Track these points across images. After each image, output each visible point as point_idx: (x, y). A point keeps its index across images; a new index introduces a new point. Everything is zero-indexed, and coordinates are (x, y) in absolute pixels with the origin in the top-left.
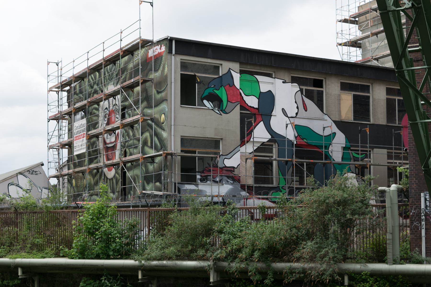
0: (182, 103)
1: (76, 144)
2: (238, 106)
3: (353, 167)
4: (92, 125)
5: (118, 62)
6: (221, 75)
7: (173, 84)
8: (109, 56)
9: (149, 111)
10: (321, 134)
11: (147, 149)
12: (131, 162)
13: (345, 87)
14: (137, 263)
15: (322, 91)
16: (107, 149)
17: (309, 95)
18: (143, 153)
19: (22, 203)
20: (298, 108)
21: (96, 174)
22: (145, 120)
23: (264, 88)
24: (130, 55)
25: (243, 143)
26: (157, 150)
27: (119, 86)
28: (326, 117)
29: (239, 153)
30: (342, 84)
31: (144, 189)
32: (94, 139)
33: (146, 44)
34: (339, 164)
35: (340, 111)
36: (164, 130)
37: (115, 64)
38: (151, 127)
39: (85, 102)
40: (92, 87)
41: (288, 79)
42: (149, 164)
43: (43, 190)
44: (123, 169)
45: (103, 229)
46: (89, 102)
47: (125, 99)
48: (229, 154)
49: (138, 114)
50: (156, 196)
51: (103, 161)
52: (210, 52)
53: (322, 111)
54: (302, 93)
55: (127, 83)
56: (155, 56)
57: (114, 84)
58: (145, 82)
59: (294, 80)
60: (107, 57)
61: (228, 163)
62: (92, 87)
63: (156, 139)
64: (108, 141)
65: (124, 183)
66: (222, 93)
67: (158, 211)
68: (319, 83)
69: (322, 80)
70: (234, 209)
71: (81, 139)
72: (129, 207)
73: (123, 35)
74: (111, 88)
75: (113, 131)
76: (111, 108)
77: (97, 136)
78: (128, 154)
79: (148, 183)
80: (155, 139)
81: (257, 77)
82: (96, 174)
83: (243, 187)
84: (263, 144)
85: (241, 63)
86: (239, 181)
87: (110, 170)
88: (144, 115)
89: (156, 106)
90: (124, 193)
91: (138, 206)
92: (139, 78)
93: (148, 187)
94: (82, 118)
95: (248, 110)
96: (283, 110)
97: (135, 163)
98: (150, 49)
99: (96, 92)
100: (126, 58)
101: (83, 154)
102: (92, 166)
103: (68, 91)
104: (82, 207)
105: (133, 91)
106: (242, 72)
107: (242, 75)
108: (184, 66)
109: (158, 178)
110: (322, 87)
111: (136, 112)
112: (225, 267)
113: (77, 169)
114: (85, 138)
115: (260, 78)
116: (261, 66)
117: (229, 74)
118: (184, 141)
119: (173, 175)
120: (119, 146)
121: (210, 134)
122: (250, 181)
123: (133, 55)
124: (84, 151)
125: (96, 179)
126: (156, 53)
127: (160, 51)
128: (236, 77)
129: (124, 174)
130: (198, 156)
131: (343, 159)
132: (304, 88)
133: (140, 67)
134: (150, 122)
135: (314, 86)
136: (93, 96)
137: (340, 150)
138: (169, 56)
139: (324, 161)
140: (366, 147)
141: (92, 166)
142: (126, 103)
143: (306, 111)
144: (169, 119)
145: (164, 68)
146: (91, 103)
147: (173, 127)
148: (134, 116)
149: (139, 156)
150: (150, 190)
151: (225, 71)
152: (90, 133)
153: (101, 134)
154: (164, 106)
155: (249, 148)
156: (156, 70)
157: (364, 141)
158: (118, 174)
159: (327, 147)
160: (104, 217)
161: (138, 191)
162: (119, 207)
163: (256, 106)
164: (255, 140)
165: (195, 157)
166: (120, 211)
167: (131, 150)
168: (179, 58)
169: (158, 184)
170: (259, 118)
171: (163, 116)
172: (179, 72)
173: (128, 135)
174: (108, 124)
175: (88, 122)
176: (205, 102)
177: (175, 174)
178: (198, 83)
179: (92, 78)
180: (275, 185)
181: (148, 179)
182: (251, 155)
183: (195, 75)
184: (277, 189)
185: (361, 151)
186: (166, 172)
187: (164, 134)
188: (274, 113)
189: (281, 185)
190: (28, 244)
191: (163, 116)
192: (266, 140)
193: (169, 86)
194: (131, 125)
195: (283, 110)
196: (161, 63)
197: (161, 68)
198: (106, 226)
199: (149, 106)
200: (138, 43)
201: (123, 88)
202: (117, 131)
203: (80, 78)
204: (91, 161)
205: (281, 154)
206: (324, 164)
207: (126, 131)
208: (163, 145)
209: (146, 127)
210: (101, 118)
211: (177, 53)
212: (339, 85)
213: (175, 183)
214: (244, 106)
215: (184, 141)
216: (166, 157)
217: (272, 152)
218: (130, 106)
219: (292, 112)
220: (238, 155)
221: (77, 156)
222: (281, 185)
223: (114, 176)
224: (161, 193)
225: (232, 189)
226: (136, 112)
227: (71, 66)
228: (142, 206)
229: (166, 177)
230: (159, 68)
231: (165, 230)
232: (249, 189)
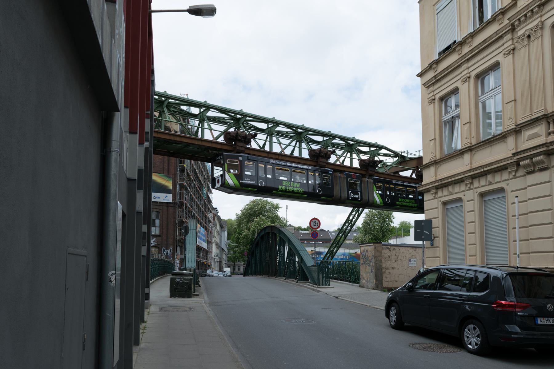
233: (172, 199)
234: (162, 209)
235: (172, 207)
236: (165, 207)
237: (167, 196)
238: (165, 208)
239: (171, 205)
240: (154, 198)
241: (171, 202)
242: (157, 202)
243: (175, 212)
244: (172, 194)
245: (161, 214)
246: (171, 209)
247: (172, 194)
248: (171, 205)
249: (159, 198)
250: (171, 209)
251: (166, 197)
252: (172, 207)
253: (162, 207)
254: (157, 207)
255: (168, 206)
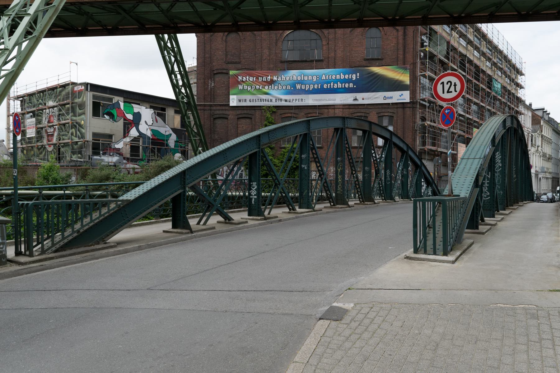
0: (93, 116)
1: (28, 131)
2: (123, 119)
3: (180, 151)
4: (39, 122)
5: (56, 90)
6: (113, 103)
7: (88, 106)
8: (51, 86)
9: (74, 118)
10: (164, 134)
11: (73, 137)
12: (64, 143)
13: (176, 112)
14: (71, 192)
15: (165, 114)
16: (48, 136)
17: (159, 115)
18: (72, 140)
19: (3, 163)
20: (153, 121)
21: (41, 148)
22: (72, 123)
23: (136, 111)
24: (63, 88)
25: (124, 137)
26: (79, 138)
27: (57, 104)
28: (167, 126)
29: (122, 142)
30: (175, 110)
31: (71, 157)
32: (39, 129)
33: (73, 84)
34: (173, 149)
35: (174, 124)
36: (83, 128)
37: (53, 91)
38: (76, 127)
39: (34, 109)
40: (38, 101)
41: (148, 106)
42: (74, 145)
43: (4, 155)
44: (59, 146)
45: (52, 176)
46: (37, 109)
47: (60, 110)
48: (118, 142)
49: (68, 119)
50: (81, 161)
51: (45, 142)
52: (108, 91)
53: (165, 123)
54: (155, 114)
55: (62, 103)
56: (78, 90)
57: (52, 101)
58: (72, 103)
59: (151, 107)
60: (49, 87)
61: (117, 146)
62: (38, 101)
63: (79, 133)
64: (49, 131)
65: (59, 154)
66: (114, 112)
67: (82, 169)
68: (164, 110)
69: (165, 108)
70: (120, 168)
71: (32, 129)
72: (64, 166)
73: (60, 77)
74: (51, 103)
75: (53, 126)
76: (51, 114)
77: (42, 128)
78: (61, 139)
79: (74, 155)
80: (78, 133)
81: (133, 105)
82: (41, 148)
83: (124, 158)
84: (135, 138)
85: (124, 98)
86: (122, 155)
87: (50, 147)
88: (72, 120)
89: (79, 116)
90: (59, 159)
91: (69, 166)
92: (69, 101)
93: (73, 157)
94: (31, 117)
95: (127, 121)
96: (146, 122)
97: (66, 145)
98: (75, 86)
99: (41, 104)
100: (61, 89)
101: (33, 137)
102: (39, 144)
103: (21, 101)
104: (40, 166)
105: (65, 107)
106: (124, 102)
107: (125, 103)
108: (94, 97)
109: (80, 153)
110: (165, 111)
111: (66, 118)
112: (115, 194)
113: (30, 145)
114: (34, 129)
115: (134, 105)
116: (134, 99)
117: (118, 103)
118: (94, 135)
119: (88, 151)
120: (56, 134)
121: (108, 132)
122: (128, 156)
123: (65, 88)
124: (34, 135)
125: (41, 151)
126: (79, 89)
127: (81, 89)
128: (122, 104)
129: (59, 149)
130: (102, 143)
131: (175, 146)
132: (156, 111)
133: (70, 96)
134: (75, 124)
135: (161, 111)
136: (38, 106)
137: (174, 142)
138: (86, 92)
139: (165, 147)
140: (186, 141)
141: (39, 144)
142: (61, 113)
143: (157, 122)
144: (86, 123)
145: (83, 98)
146: (38, 110)
147: (88, 127)
148: (66, 120)
149: (70, 141)
150: (74, 158)
151: (116, 101)
152: (37, 126)
153: (46, 127)
154: (83, 116)
155: (128, 140)
156: (79, 98)
157: (185, 139)
158: (55, 149)
159: (167, 141)
160: (53, 171)
161: (68, 158)
162: (61, 166)
163: (132, 119)
164: (131, 136)
165: (100, 143)
166: (61, 168)
167: (64, 137)
168: (92, 93)
169: (79, 155)
170: (133, 125)
171: (83, 122)
172: (92, 100)
173: (62, 129)
174: (49, 122)
175: (36, 120)
176: (105, 116)
177: (89, 151)
178: (101, 106)
179: (38, 96)
180: (141, 157)
181: (73, 153)
182: (129, 143)
183: (100, 102)
184: (142, 160)
185: (184, 143)
186: (84, 149)
187: (83, 131)
188: (140, 123)
189: (144, 158)
190: (8, 183)
191: (83, 122)
192: (136, 136)
193: (86, 107)
194: (64, 125)
195: (146, 122)
196: (81, 95)
197: (82, 97)
198: (55, 175)
199: (75, 116)
200: (69, 83)
201: (59, 105)
202: (54, 127)
203: (31, 95)
204: (38, 141)
205: (144, 143)
206: (166, 149)
207: (60, 127)
208: (83, 136)
209: (73, 126)
210: (44, 119)
211: (91, 90)
212: (174, 111)
213: (89, 156)
214: (125, 119)
215: (94, 135)
216: (84, 142)
217: (139, 142)
218: (63, 115)
219: (150, 122)
220: (122, 143)
221: (29, 138)
222: (144, 158)
223: (53, 150)
224: (82, 160)
225: (118, 160)
226: (66, 118)
227: (25, 87)
228: (71, 166)
229: (85, 152)
230: (81, 96)
231: (86, 177)
232: (128, 159)
233: (410, 97)
234: (395, 112)
235: (410, 108)
236: (401, 109)
237: (402, 95)
238: (400, 110)
239: (409, 105)
240: (385, 98)
241: (409, 101)
242: (389, 104)
243: (414, 115)
244: (409, 91)
245: (395, 118)
246: (408, 111)
247: (409, 91)
248: (409, 105)
249: (391, 98)
250: (408, 111)
251: (400, 96)
252: (410, 108)
253: (396, 109)
254: (389, 110)
255: (404, 108)
